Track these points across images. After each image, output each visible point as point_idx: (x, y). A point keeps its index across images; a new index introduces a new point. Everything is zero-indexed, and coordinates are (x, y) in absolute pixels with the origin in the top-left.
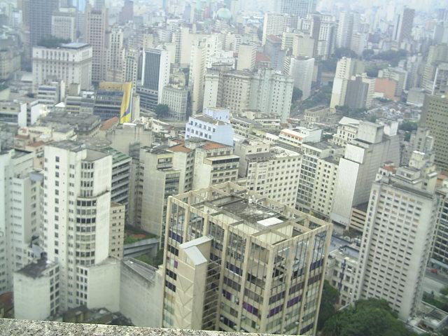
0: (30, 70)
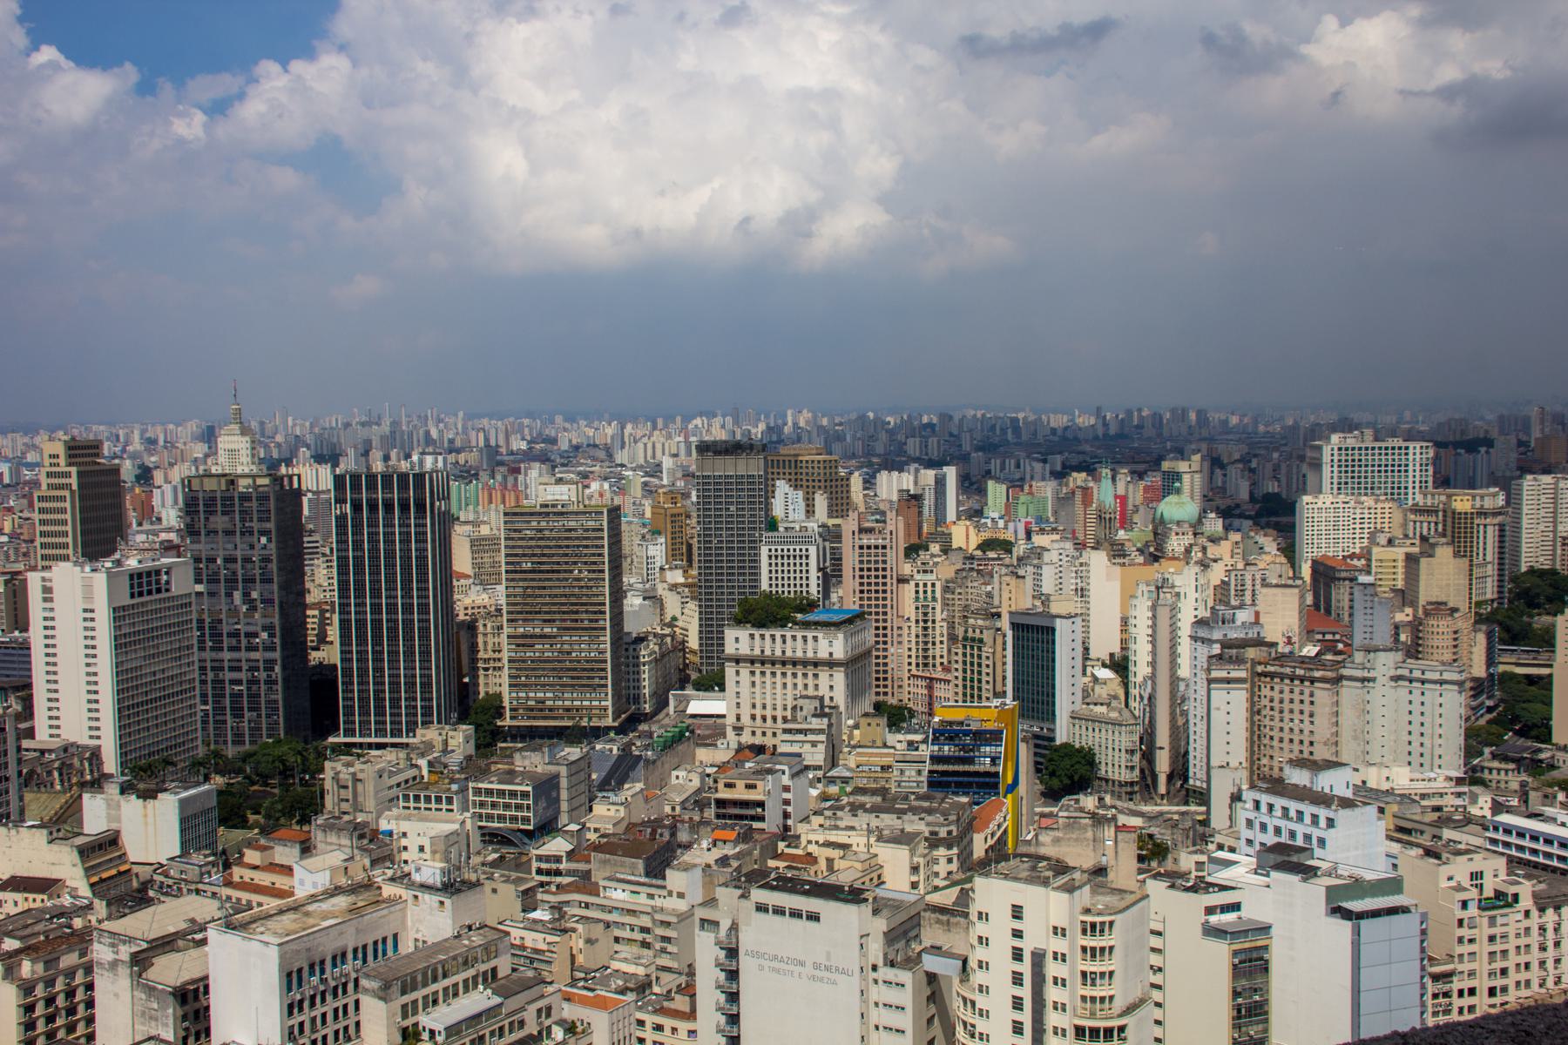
0: (713, 683)
